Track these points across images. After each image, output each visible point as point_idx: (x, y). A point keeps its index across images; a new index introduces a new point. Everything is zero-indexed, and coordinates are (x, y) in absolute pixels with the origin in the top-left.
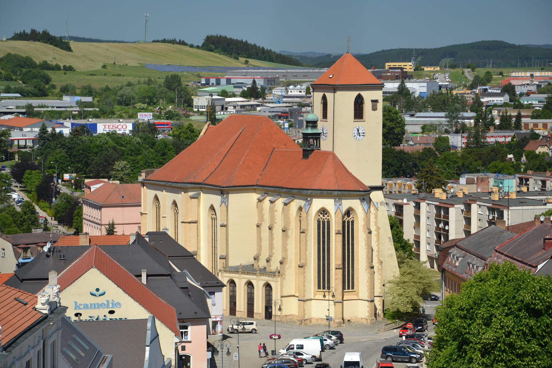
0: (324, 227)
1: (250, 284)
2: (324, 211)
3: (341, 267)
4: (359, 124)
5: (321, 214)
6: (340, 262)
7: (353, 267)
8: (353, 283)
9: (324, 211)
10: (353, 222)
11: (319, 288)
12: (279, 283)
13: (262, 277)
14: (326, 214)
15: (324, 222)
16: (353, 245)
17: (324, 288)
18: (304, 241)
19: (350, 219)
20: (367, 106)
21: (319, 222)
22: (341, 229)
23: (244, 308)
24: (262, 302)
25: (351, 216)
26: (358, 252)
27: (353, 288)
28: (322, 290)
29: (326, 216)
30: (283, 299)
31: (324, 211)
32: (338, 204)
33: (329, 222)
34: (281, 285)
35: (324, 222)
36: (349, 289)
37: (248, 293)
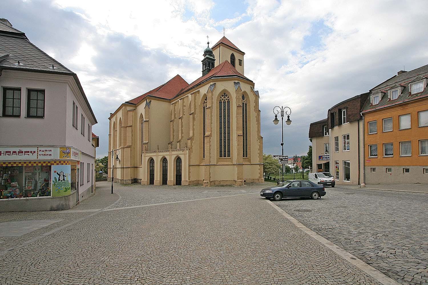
1: (164, 160)
2: (225, 94)
3: (242, 134)
5: (223, 96)
9: (225, 94)
11: (221, 156)
12: (187, 155)
13: (173, 153)
14: (227, 96)
15: (224, 102)
18: (210, 115)
20: (237, 62)
21: (220, 103)
23: (160, 178)
24: (174, 172)
28: (223, 157)
31: (225, 94)
33: (229, 102)
34: (189, 156)
35: (224, 102)
37: (163, 166)
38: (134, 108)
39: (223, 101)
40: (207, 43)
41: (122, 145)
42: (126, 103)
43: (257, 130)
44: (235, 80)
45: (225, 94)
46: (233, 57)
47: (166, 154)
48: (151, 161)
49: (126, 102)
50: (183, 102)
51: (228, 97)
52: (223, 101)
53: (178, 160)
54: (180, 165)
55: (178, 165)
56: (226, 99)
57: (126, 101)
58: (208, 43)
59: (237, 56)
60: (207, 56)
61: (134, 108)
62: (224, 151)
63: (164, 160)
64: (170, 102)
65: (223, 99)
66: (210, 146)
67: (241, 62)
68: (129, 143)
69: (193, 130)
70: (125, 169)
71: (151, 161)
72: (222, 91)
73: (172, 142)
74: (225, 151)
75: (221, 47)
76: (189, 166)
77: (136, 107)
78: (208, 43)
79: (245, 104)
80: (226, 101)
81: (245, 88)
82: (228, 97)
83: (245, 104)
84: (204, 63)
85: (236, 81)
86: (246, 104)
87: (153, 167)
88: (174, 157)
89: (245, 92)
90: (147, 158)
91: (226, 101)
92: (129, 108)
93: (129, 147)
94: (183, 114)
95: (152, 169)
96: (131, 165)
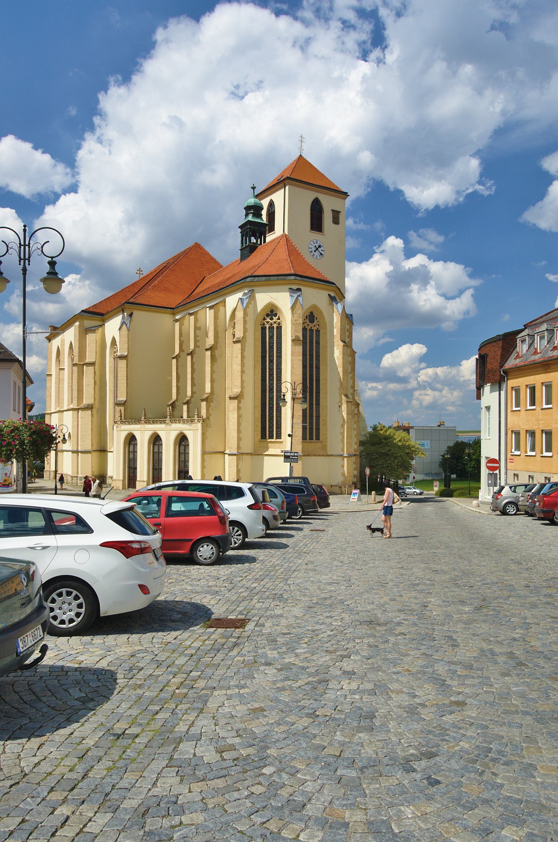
0: (271, 338)
1: (156, 440)
4: (315, 235)
5: (268, 315)
7: (318, 404)
8: (318, 429)
9: (272, 311)
10: (318, 331)
13: (174, 426)
14: (276, 315)
15: (271, 328)
16: (318, 368)
17: (271, 437)
18: (240, 356)
19: (313, 326)
20: (327, 217)
21: (263, 329)
22: (300, 335)
25: (316, 322)
26: (326, 379)
27: (318, 438)
29: (275, 319)
30: (206, 456)
31: (272, 311)
32: (295, 295)
33: (279, 328)
34: (203, 434)
35: (271, 328)
36: (311, 438)
38: (99, 323)
39: (267, 326)
40: (252, 188)
41: (75, 402)
42: (85, 314)
43: (339, 386)
44: (293, 284)
45: (272, 311)
46: (316, 210)
47: (160, 429)
48: (131, 440)
49: (82, 311)
50: (196, 321)
51: (279, 319)
52: (267, 326)
54: (186, 452)
55: (182, 451)
56: (275, 323)
57: (84, 309)
58: (254, 188)
59: (328, 203)
60: (250, 218)
61: (99, 323)
62: (268, 428)
63: (156, 440)
64: (174, 314)
65: (268, 322)
66: (239, 416)
68: (88, 399)
69: (212, 381)
70: (80, 454)
71: (131, 440)
72: (266, 307)
73: (174, 402)
74: (271, 427)
75: (287, 188)
76: (204, 453)
77: (104, 321)
78: (254, 188)
79: (314, 332)
80: (275, 326)
82: (279, 319)
83: (314, 332)
84: (244, 231)
85: (295, 287)
86: (319, 331)
87: (135, 452)
88: (173, 435)
89: (315, 307)
90: (123, 435)
91: (275, 326)
92: (88, 323)
93: (89, 407)
94: (196, 346)
95: (132, 456)
96: (92, 445)
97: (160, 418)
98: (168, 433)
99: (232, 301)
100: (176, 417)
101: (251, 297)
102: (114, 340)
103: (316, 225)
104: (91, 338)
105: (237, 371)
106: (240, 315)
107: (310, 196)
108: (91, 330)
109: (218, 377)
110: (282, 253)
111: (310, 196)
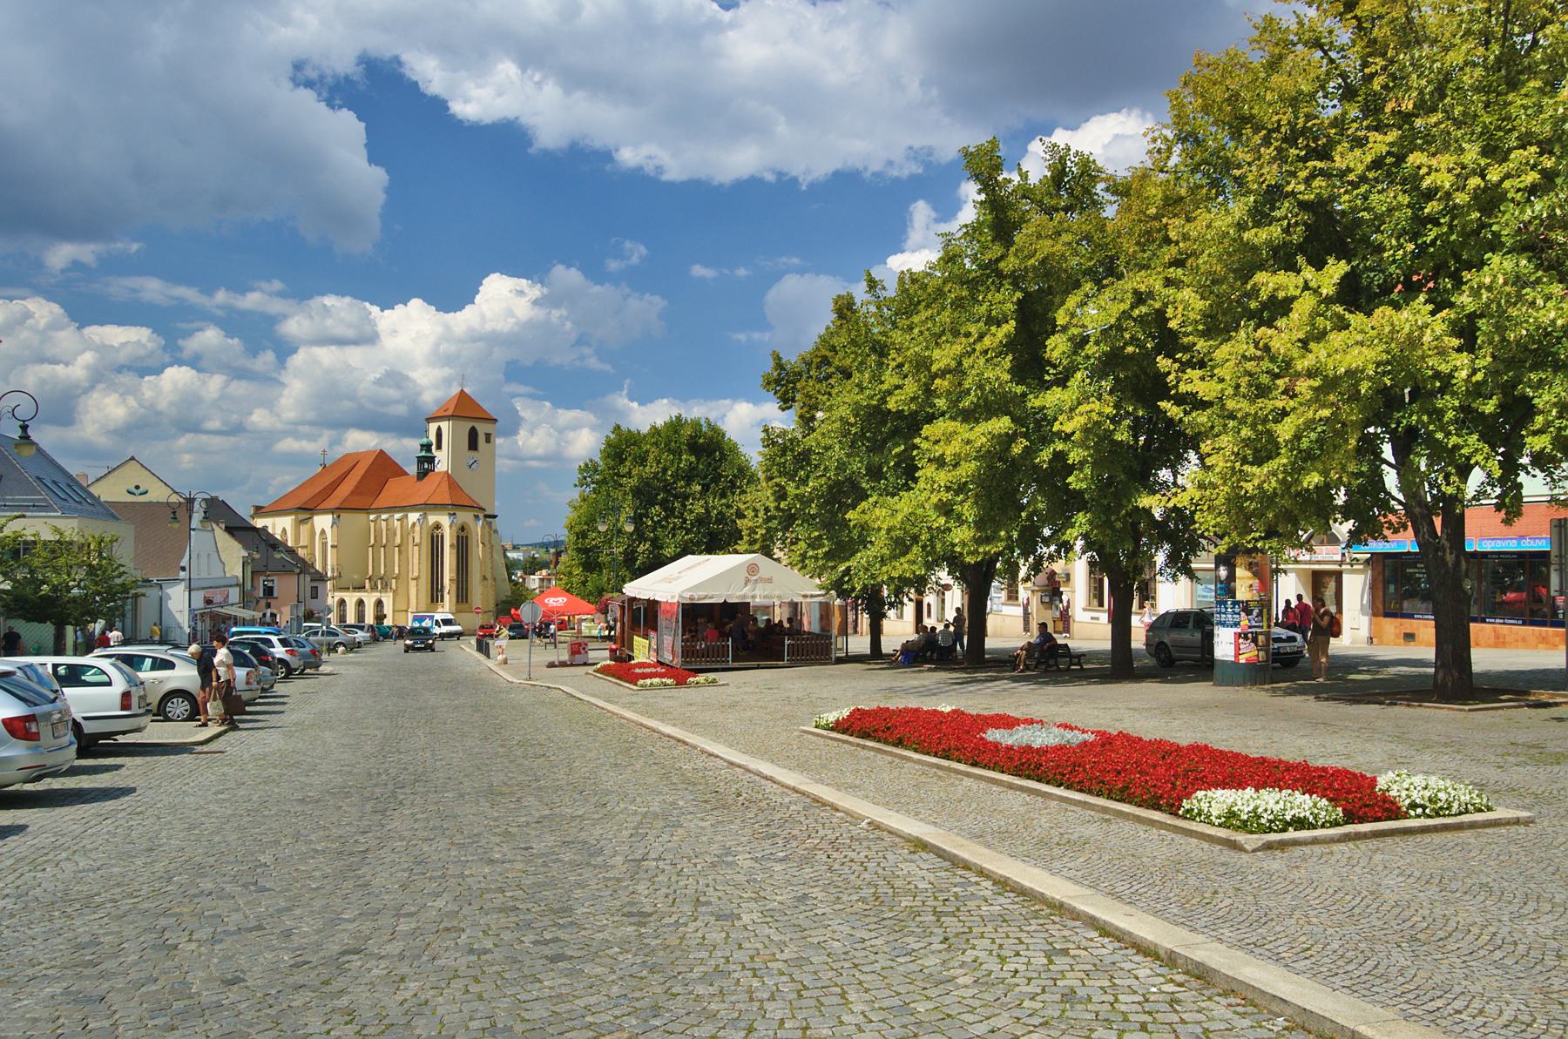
1: (360, 603)
2: (438, 526)
4: (473, 453)
6: (454, 575)
31: (438, 526)
53: (379, 603)
59: (482, 429)
62: (436, 595)
63: (360, 603)
67: (488, 438)
81: (465, 517)
97: (362, 588)
98: (370, 599)
99: (413, 517)
100: (374, 588)
101: (425, 516)
102: (323, 532)
103: (473, 444)
104: (304, 529)
105: (418, 563)
106: (417, 528)
107: (468, 425)
108: (303, 521)
109: (405, 562)
110: (445, 486)
111: (468, 425)
